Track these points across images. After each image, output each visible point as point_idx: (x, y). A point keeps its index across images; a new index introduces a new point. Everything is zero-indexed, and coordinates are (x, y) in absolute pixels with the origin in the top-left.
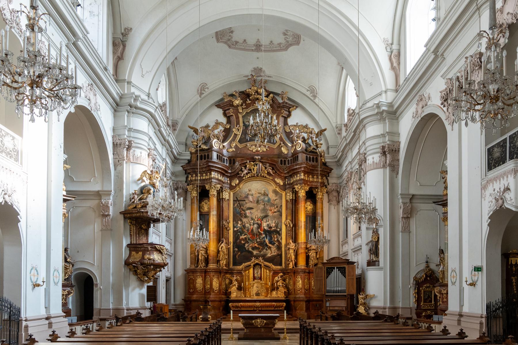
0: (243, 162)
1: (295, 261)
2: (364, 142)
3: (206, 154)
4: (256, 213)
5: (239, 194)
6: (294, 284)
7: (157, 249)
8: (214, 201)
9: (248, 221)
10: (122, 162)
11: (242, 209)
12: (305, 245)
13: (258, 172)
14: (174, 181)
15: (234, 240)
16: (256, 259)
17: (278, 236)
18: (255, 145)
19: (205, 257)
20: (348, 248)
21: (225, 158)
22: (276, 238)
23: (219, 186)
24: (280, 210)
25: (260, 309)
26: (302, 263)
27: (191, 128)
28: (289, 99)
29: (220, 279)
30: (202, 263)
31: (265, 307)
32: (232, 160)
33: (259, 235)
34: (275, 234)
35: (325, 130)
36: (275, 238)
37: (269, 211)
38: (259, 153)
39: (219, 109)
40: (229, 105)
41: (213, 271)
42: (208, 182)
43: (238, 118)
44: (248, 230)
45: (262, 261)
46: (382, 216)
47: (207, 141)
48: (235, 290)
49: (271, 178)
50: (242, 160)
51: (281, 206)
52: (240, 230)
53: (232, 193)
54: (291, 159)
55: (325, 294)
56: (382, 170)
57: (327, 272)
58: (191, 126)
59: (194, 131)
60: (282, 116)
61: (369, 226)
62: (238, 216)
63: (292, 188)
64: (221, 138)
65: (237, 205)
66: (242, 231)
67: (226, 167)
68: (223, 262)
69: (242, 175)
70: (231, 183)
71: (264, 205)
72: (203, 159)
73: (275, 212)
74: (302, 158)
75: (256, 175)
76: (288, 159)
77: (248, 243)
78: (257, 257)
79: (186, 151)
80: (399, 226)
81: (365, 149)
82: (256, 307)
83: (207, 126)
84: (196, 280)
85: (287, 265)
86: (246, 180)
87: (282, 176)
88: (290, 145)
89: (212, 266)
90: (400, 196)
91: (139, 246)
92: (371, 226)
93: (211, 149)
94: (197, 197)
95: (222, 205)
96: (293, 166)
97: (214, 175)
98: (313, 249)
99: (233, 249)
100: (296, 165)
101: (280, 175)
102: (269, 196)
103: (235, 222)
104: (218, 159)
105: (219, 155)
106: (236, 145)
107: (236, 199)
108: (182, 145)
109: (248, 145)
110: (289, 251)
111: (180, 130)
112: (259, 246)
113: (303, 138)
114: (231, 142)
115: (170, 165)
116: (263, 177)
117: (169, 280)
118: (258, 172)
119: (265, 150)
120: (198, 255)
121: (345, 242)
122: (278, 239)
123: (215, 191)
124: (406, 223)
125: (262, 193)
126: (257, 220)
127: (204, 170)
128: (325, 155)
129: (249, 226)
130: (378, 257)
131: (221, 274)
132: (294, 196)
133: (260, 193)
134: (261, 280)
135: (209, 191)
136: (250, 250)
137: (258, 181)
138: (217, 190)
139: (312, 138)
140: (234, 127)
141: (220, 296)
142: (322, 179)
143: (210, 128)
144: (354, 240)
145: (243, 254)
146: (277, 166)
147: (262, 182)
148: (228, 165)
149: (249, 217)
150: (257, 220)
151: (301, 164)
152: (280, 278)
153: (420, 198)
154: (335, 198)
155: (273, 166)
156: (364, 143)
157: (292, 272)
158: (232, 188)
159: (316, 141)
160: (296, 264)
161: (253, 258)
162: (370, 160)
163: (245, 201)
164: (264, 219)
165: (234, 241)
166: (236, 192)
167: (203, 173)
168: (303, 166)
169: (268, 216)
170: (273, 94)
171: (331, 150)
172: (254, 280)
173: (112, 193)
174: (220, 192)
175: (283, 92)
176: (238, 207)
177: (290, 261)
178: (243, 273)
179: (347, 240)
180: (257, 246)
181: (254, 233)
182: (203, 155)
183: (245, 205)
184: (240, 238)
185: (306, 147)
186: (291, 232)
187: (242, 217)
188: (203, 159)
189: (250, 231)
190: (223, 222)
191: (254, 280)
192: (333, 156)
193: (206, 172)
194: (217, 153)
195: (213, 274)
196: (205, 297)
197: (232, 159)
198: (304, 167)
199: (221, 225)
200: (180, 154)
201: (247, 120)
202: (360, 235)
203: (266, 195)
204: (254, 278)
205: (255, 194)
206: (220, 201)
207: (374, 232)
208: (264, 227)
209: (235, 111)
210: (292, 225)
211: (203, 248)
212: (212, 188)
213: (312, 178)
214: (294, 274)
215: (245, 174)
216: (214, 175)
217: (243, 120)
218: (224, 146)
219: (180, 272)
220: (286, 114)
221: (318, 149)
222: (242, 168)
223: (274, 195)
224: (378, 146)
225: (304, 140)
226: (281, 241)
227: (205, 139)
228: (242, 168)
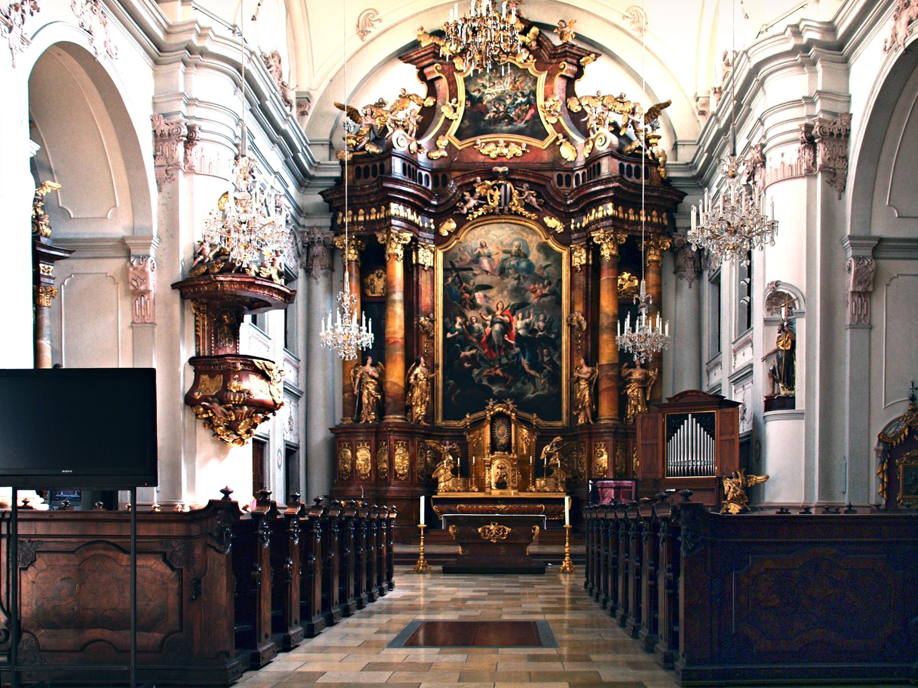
0: (466, 181)
1: (591, 410)
2: (760, 119)
3: (378, 164)
4: (498, 299)
5: (456, 254)
7: (258, 369)
8: (397, 270)
9: (479, 317)
10: (175, 172)
11: (465, 288)
12: (616, 369)
13: (503, 205)
14: (304, 226)
16: (497, 403)
17: (552, 350)
18: (493, 142)
19: (377, 398)
20: (720, 378)
21: (424, 173)
22: (547, 356)
23: (408, 236)
24: (558, 290)
26: (606, 410)
27: (341, 107)
28: (578, 37)
30: (369, 414)
32: (440, 174)
35: (667, 104)
37: (529, 292)
38: (504, 160)
39: (409, 65)
40: (431, 55)
41: (395, 429)
42: (383, 225)
43: (452, 83)
45: (511, 406)
46: (804, 290)
47: (380, 136)
49: (534, 216)
50: (464, 177)
51: (560, 281)
53: (440, 254)
54: (584, 174)
55: (664, 477)
56: (803, 182)
57: (668, 426)
58: (343, 102)
59: (348, 115)
60: (562, 76)
61: (771, 317)
62: (455, 305)
63: (585, 239)
64: (413, 127)
65: (453, 281)
66: (466, 338)
67: (423, 193)
68: (420, 410)
69: (465, 211)
70: (437, 228)
71: (518, 278)
72: (371, 176)
73: (545, 295)
74: (607, 167)
75: (497, 211)
76: (577, 172)
77: (480, 367)
78: (500, 399)
79: (330, 160)
80: (846, 314)
81: (764, 137)
83: (381, 104)
85: (573, 419)
86: (475, 221)
87: (561, 212)
88: (580, 141)
89: (394, 418)
90: (848, 242)
91: (217, 362)
92: (776, 316)
93: (389, 151)
94: (356, 261)
95: (418, 279)
96: (589, 187)
97: (396, 209)
98: (637, 380)
100: (595, 184)
101: (557, 210)
102: (531, 258)
103: (447, 320)
104: (404, 172)
105: (407, 164)
106: (450, 143)
107: (450, 266)
108: (321, 148)
109: (479, 142)
110: (579, 384)
111: (316, 114)
112: (506, 375)
113: (614, 124)
114: (436, 137)
115: (292, 189)
116: (516, 214)
118: (503, 205)
119: (519, 153)
120: (361, 394)
121: (715, 362)
122: (552, 358)
123: (400, 247)
124: (862, 305)
125: (513, 252)
126: (502, 315)
127: (372, 200)
128: (667, 162)
129: (481, 327)
130: (793, 389)
132: (590, 257)
134: (510, 452)
135: (384, 246)
136: (485, 383)
137: (503, 225)
138: (404, 245)
139: (635, 125)
140: (444, 104)
142: (659, 216)
143: (388, 108)
144: (735, 355)
146: (548, 187)
147: (513, 226)
148: (430, 187)
150: (502, 315)
151: (608, 180)
153: (895, 248)
154: (690, 263)
155: (539, 189)
156: (761, 121)
158: (440, 240)
159: (646, 130)
160: (595, 415)
161: (491, 400)
162: (774, 159)
163: (471, 269)
164: (517, 312)
166: (451, 249)
167: (371, 208)
168: (611, 185)
170: (539, 28)
171: (681, 150)
172: (492, 453)
173: (153, 242)
174: (410, 250)
175: (563, 21)
176: (456, 284)
177: (580, 407)
178: (468, 437)
179: (719, 357)
180: (501, 374)
181: (494, 344)
182: (370, 166)
183: (472, 279)
184: (461, 355)
185: (620, 143)
186: (584, 342)
188: (371, 176)
189: (484, 339)
190: (419, 319)
192: (687, 164)
193: (376, 204)
194: (403, 161)
195: (396, 437)
196: (377, 491)
197: (440, 175)
198: (615, 189)
199: (415, 326)
200: (316, 165)
201: (476, 88)
202: (749, 342)
203: (522, 255)
204: (494, 447)
205: (497, 254)
206: (413, 270)
207: (782, 329)
208: (517, 330)
209: (446, 68)
210: (584, 327)
211: (372, 377)
212: (393, 239)
213: (634, 215)
215: (470, 209)
216: (396, 209)
217: (466, 86)
218: (419, 147)
219: (320, 434)
220: (571, 72)
221: (650, 148)
222: (465, 193)
223: (541, 256)
224: (795, 125)
225: (616, 129)
226: (558, 363)
227: (374, 132)
228: (464, 196)
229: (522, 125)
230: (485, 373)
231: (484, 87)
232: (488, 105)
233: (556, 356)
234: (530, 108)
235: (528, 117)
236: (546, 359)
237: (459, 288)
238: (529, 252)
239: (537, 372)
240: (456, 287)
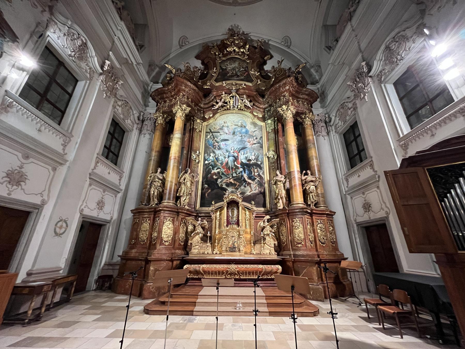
5: (213, 126)
6: (291, 232)
9: (222, 154)
11: (215, 141)
15: (204, 175)
17: (259, 170)
24: (261, 141)
29: (177, 223)
31: (246, 274)
33: (235, 169)
34: (255, 168)
36: (255, 172)
44: (222, 164)
48: (198, 242)
52: (212, 163)
62: (211, 148)
65: (210, 137)
73: (255, 144)
77: (222, 178)
82: (229, 274)
84: (142, 224)
87: (261, 108)
99: (203, 185)
102: (246, 128)
103: (206, 155)
112: (235, 182)
117: (105, 225)
122: (259, 174)
125: (239, 125)
129: (223, 158)
131: (178, 215)
133: (237, 125)
136: (224, 186)
141: (173, 251)
145: (215, 191)
149: (223, 149)
152: (267, 224)
157: (284, 213)
163: (219, 132)
165: (204, 176)
169: (246, 148)
172: (227, 226)
176: (211, 139)
180: (233, 182)
186: (276, 164)
187: (215, 149)
191: (227, 226)
203: (243, 126)
204: (228, 223)
214: (288, 216)
223: (252, 126)
226: (262, 176)
229: (243, 78)
230: (224, 181)
231: (228, 65)
232: (229, 71)
234: (246, 72)
235: (245, 75)
236: (256, 174)
237: (213, 140)
238: (246, 125)
239: (252, 180)
240: (212, 140)
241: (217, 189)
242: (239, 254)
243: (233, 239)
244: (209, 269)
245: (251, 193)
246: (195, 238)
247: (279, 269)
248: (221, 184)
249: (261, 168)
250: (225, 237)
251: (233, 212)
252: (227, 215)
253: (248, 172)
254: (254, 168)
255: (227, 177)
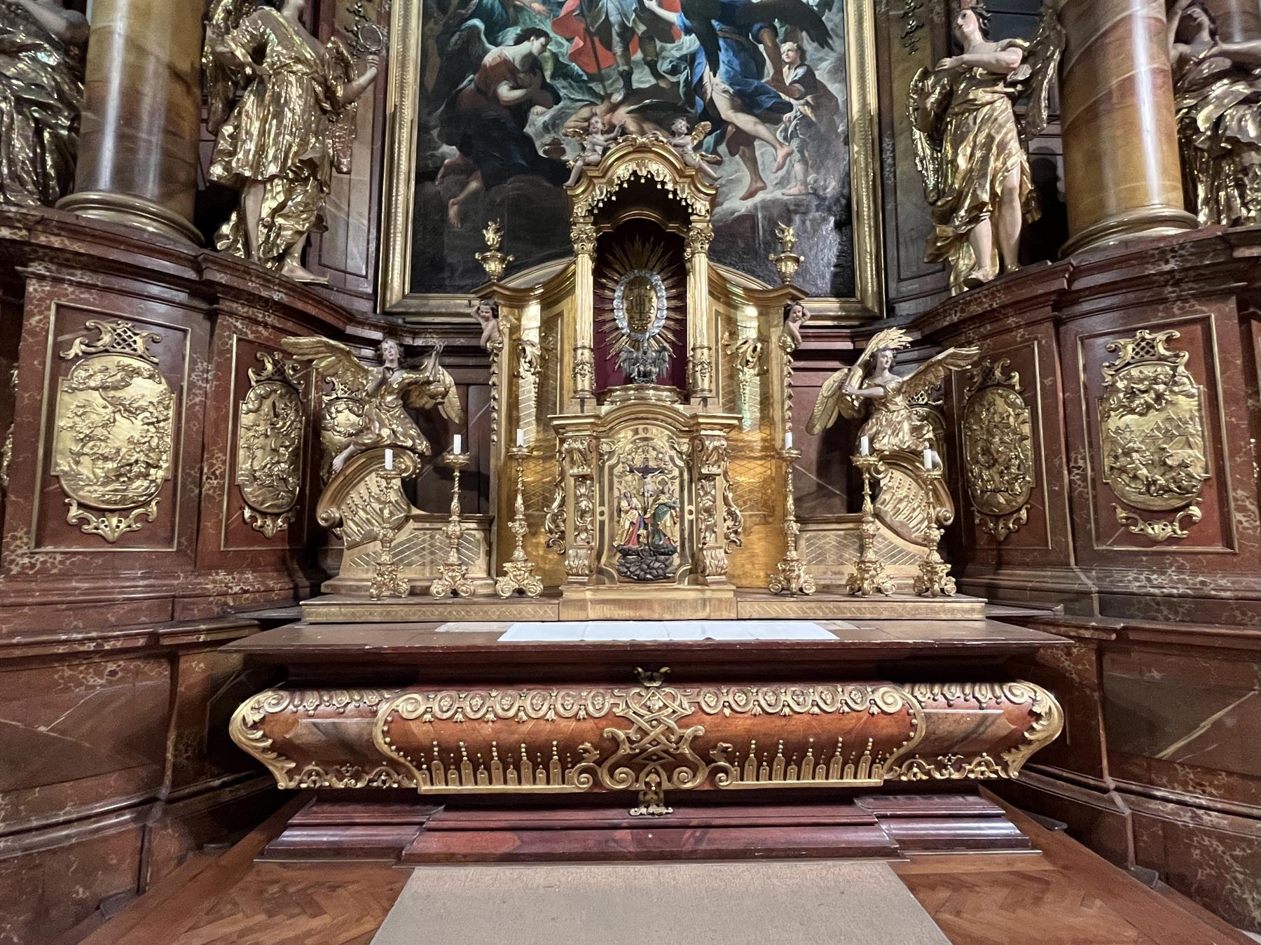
17: (809, 46)
25: (690, 782)
34: (781, 31)
77: (558, 99)
82: (628, 761)
99: (424, 145)
122: (810, 73)
165: (431, 82)
181: (607, 23)
184: (488, 60)
191: (600, 395)
226: (833, 88)
233: (826, 65)
236: (790, 75)
241: (521, 170)
242: (692, 595)
243: (651, 484)
244: (448, 731)
245: (750, 203)
246: (362, 488)
247: (1038, 717)
248: (548, 139)
249: (822, 36)
250: (586, 470)
251: (638, 311)
252: (598, 324)
253: (736, 63)
254: (775, 32)
255: (590, 90)
